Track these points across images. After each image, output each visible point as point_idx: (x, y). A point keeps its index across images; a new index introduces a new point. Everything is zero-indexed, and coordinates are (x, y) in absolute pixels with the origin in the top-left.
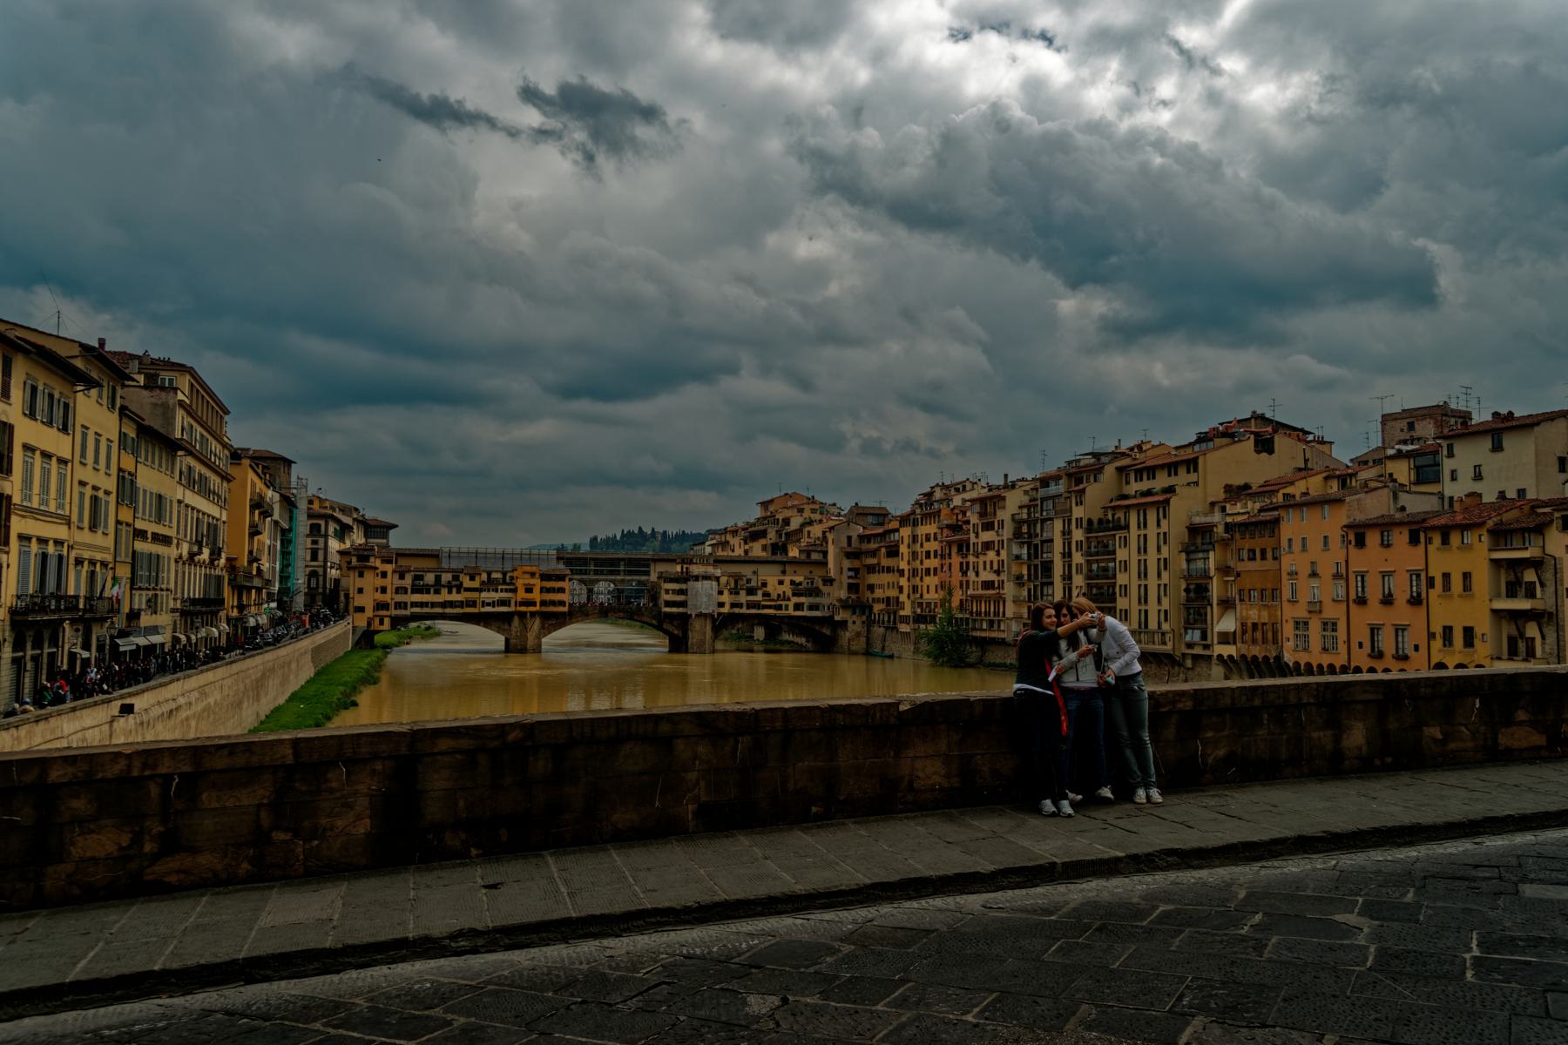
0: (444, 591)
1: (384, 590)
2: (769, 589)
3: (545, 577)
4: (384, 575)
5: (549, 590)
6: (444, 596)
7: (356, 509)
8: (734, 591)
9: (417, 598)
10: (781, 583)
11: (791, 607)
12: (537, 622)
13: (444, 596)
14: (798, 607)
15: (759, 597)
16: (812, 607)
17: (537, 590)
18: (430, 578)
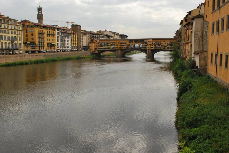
0: (105, 46)
1: (96, 46)
2: (163, 44)
3: (121, 43)
4: (96, 44)
5: (122, 46)
6: (105, 47)
7: (117, 33)
8: (155, 45)
9: (101, 47)
10: (165, 43)
11: (167, 48)
12: (120, 51)
13: (105, 47)
14: (168, 48)
15: (160, 46)
16: (171, 48)
17: (118, 45)
18: (103, 44)
